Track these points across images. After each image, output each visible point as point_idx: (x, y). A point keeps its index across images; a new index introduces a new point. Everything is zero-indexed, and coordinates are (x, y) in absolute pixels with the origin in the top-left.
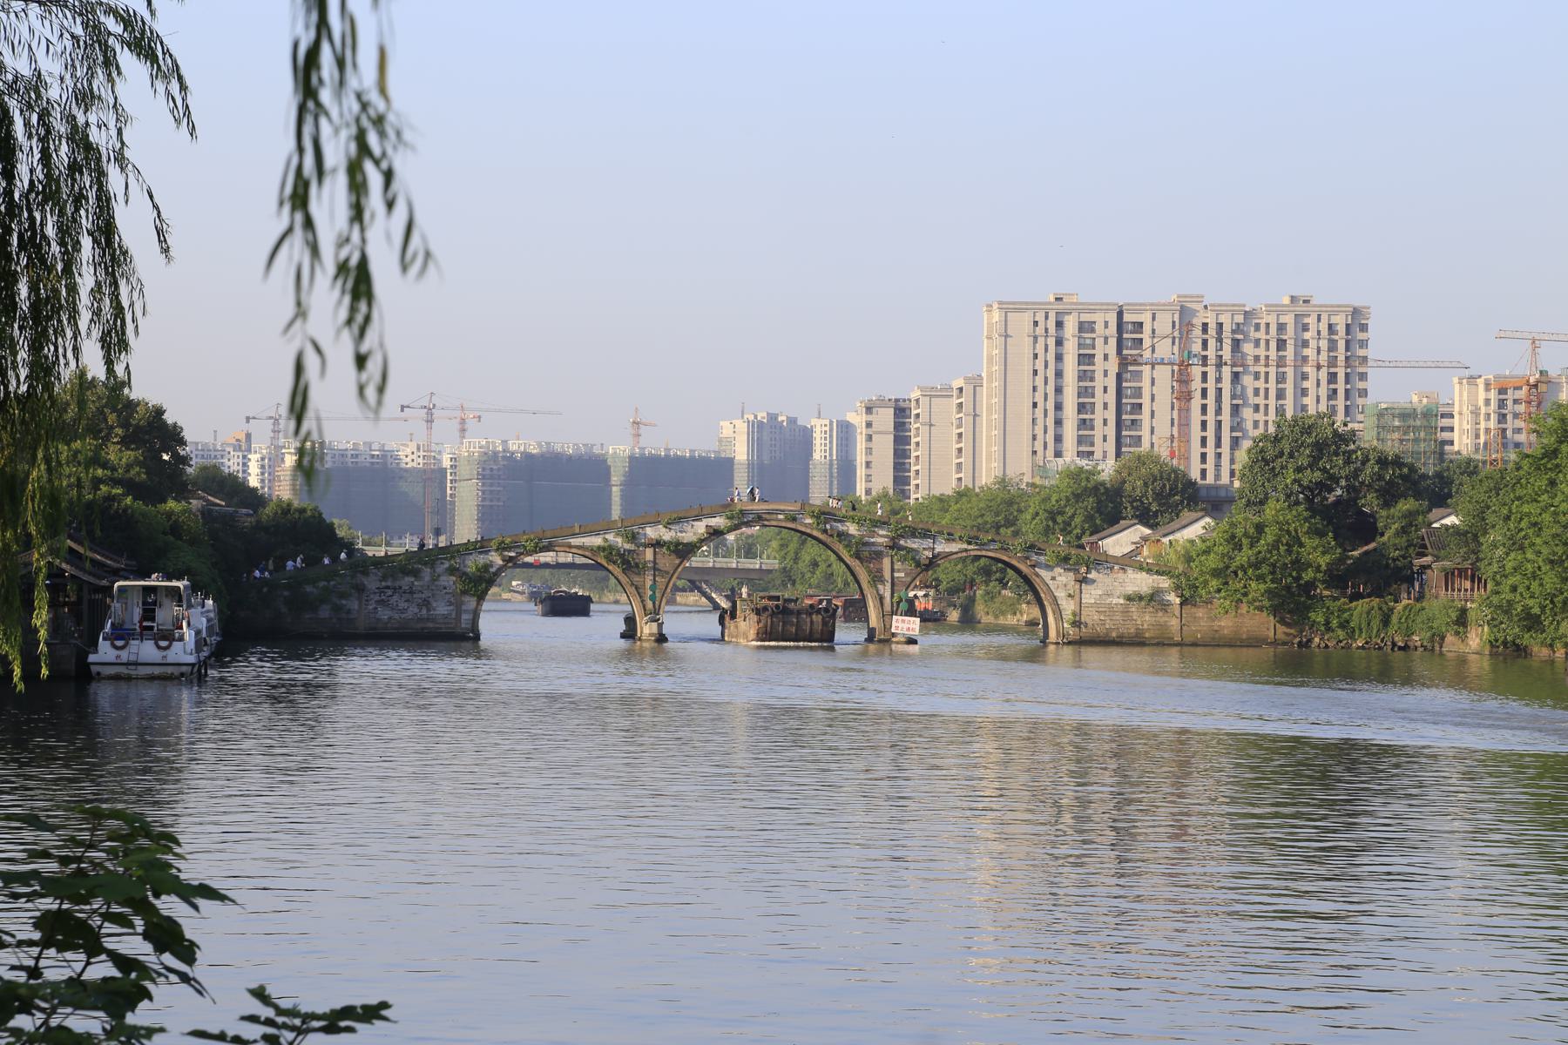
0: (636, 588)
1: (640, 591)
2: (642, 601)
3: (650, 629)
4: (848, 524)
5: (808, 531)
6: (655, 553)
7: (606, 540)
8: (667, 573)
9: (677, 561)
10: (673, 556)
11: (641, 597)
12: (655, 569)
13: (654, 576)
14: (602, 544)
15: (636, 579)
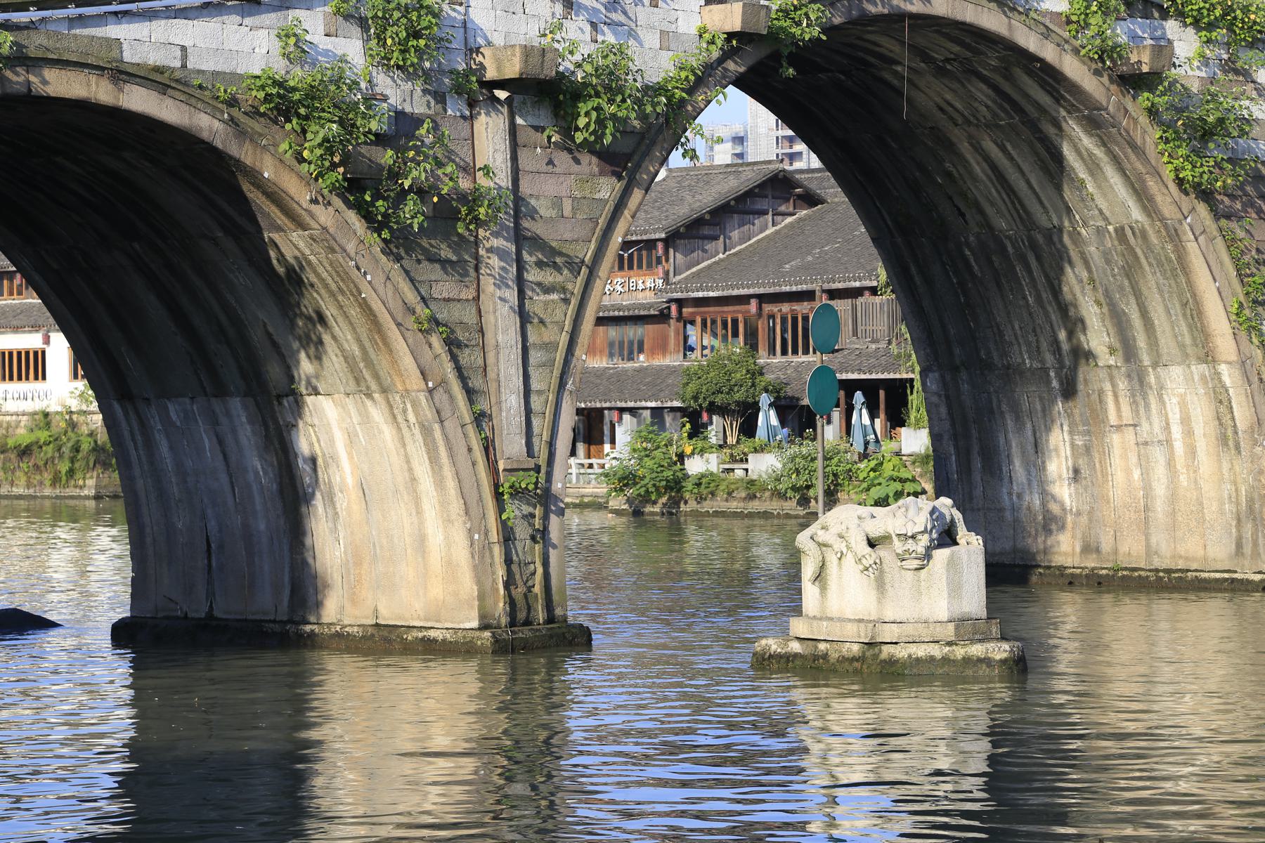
0: (452, 344)
1: (465, 357)
2: (480, 418)
3: (955, 589)
4: (1172, 27)
5: (1049, 53)
6: (513, 130)
7: (298, 49)
8: (574, 266)
9: (608, 189)
10: (589, 163)
11: (470, 393)
12: (520, 238)
13: (520, 281)
14: (279, 67)
15: (445, 287)
